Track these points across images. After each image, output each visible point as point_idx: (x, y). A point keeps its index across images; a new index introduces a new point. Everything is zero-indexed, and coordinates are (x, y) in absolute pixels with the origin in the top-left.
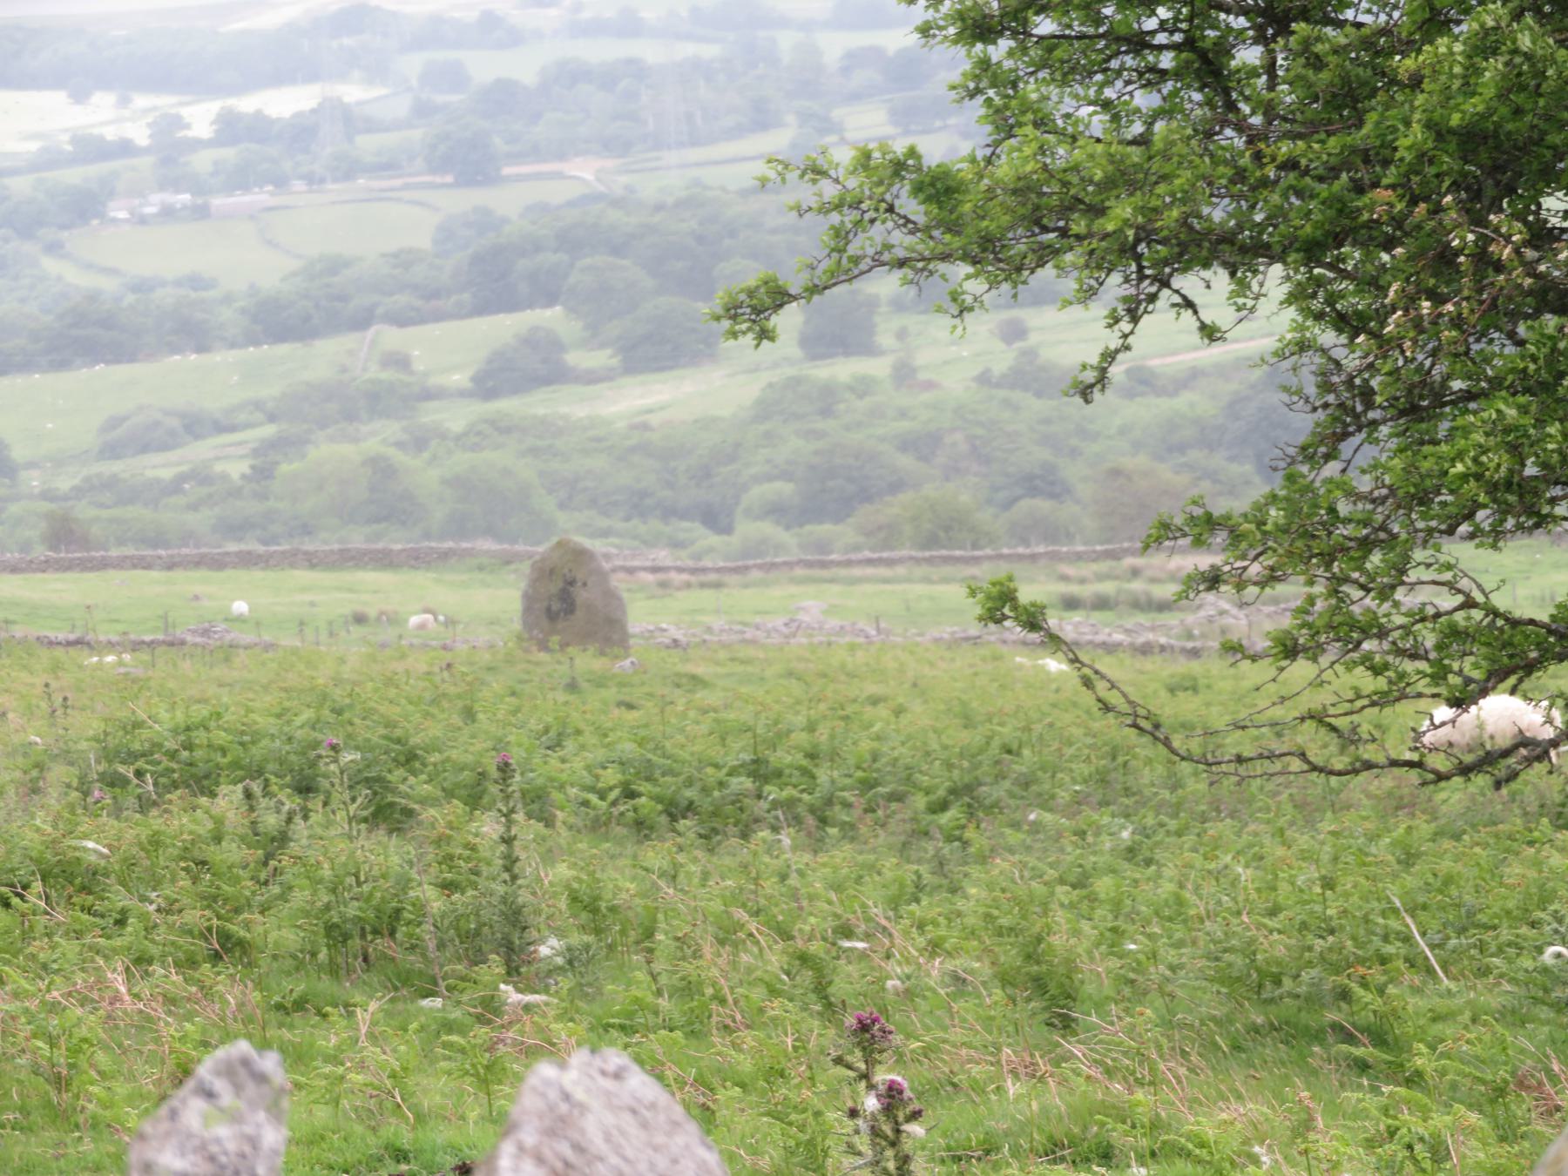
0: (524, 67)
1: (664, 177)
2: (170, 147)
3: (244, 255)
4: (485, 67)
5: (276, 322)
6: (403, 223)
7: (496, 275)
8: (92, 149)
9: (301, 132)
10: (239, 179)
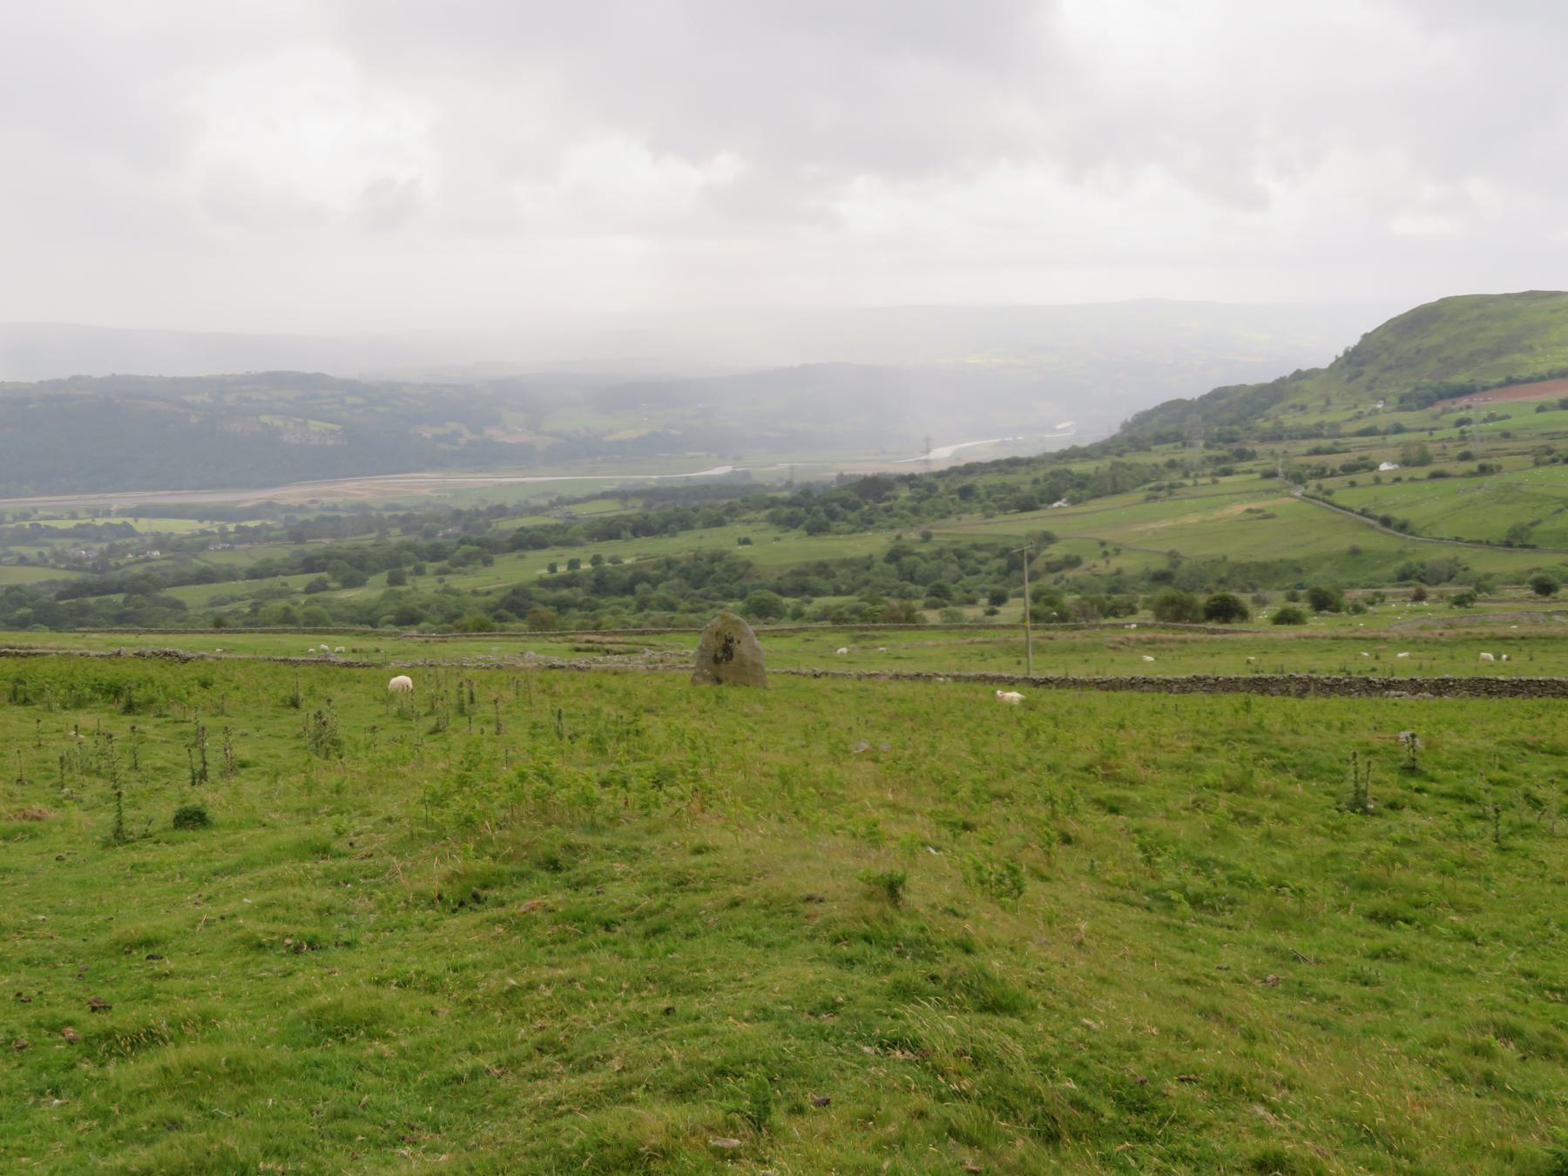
0: (311, 517)
1: (348, 542)
2: (224, 533)
3: (242, 559)
4: (300, 517)
5: (253, 574)
6: (281, 553)
7: (309, 565)
8: (203, 533)
9: (256, 530)
10: (241, 541)
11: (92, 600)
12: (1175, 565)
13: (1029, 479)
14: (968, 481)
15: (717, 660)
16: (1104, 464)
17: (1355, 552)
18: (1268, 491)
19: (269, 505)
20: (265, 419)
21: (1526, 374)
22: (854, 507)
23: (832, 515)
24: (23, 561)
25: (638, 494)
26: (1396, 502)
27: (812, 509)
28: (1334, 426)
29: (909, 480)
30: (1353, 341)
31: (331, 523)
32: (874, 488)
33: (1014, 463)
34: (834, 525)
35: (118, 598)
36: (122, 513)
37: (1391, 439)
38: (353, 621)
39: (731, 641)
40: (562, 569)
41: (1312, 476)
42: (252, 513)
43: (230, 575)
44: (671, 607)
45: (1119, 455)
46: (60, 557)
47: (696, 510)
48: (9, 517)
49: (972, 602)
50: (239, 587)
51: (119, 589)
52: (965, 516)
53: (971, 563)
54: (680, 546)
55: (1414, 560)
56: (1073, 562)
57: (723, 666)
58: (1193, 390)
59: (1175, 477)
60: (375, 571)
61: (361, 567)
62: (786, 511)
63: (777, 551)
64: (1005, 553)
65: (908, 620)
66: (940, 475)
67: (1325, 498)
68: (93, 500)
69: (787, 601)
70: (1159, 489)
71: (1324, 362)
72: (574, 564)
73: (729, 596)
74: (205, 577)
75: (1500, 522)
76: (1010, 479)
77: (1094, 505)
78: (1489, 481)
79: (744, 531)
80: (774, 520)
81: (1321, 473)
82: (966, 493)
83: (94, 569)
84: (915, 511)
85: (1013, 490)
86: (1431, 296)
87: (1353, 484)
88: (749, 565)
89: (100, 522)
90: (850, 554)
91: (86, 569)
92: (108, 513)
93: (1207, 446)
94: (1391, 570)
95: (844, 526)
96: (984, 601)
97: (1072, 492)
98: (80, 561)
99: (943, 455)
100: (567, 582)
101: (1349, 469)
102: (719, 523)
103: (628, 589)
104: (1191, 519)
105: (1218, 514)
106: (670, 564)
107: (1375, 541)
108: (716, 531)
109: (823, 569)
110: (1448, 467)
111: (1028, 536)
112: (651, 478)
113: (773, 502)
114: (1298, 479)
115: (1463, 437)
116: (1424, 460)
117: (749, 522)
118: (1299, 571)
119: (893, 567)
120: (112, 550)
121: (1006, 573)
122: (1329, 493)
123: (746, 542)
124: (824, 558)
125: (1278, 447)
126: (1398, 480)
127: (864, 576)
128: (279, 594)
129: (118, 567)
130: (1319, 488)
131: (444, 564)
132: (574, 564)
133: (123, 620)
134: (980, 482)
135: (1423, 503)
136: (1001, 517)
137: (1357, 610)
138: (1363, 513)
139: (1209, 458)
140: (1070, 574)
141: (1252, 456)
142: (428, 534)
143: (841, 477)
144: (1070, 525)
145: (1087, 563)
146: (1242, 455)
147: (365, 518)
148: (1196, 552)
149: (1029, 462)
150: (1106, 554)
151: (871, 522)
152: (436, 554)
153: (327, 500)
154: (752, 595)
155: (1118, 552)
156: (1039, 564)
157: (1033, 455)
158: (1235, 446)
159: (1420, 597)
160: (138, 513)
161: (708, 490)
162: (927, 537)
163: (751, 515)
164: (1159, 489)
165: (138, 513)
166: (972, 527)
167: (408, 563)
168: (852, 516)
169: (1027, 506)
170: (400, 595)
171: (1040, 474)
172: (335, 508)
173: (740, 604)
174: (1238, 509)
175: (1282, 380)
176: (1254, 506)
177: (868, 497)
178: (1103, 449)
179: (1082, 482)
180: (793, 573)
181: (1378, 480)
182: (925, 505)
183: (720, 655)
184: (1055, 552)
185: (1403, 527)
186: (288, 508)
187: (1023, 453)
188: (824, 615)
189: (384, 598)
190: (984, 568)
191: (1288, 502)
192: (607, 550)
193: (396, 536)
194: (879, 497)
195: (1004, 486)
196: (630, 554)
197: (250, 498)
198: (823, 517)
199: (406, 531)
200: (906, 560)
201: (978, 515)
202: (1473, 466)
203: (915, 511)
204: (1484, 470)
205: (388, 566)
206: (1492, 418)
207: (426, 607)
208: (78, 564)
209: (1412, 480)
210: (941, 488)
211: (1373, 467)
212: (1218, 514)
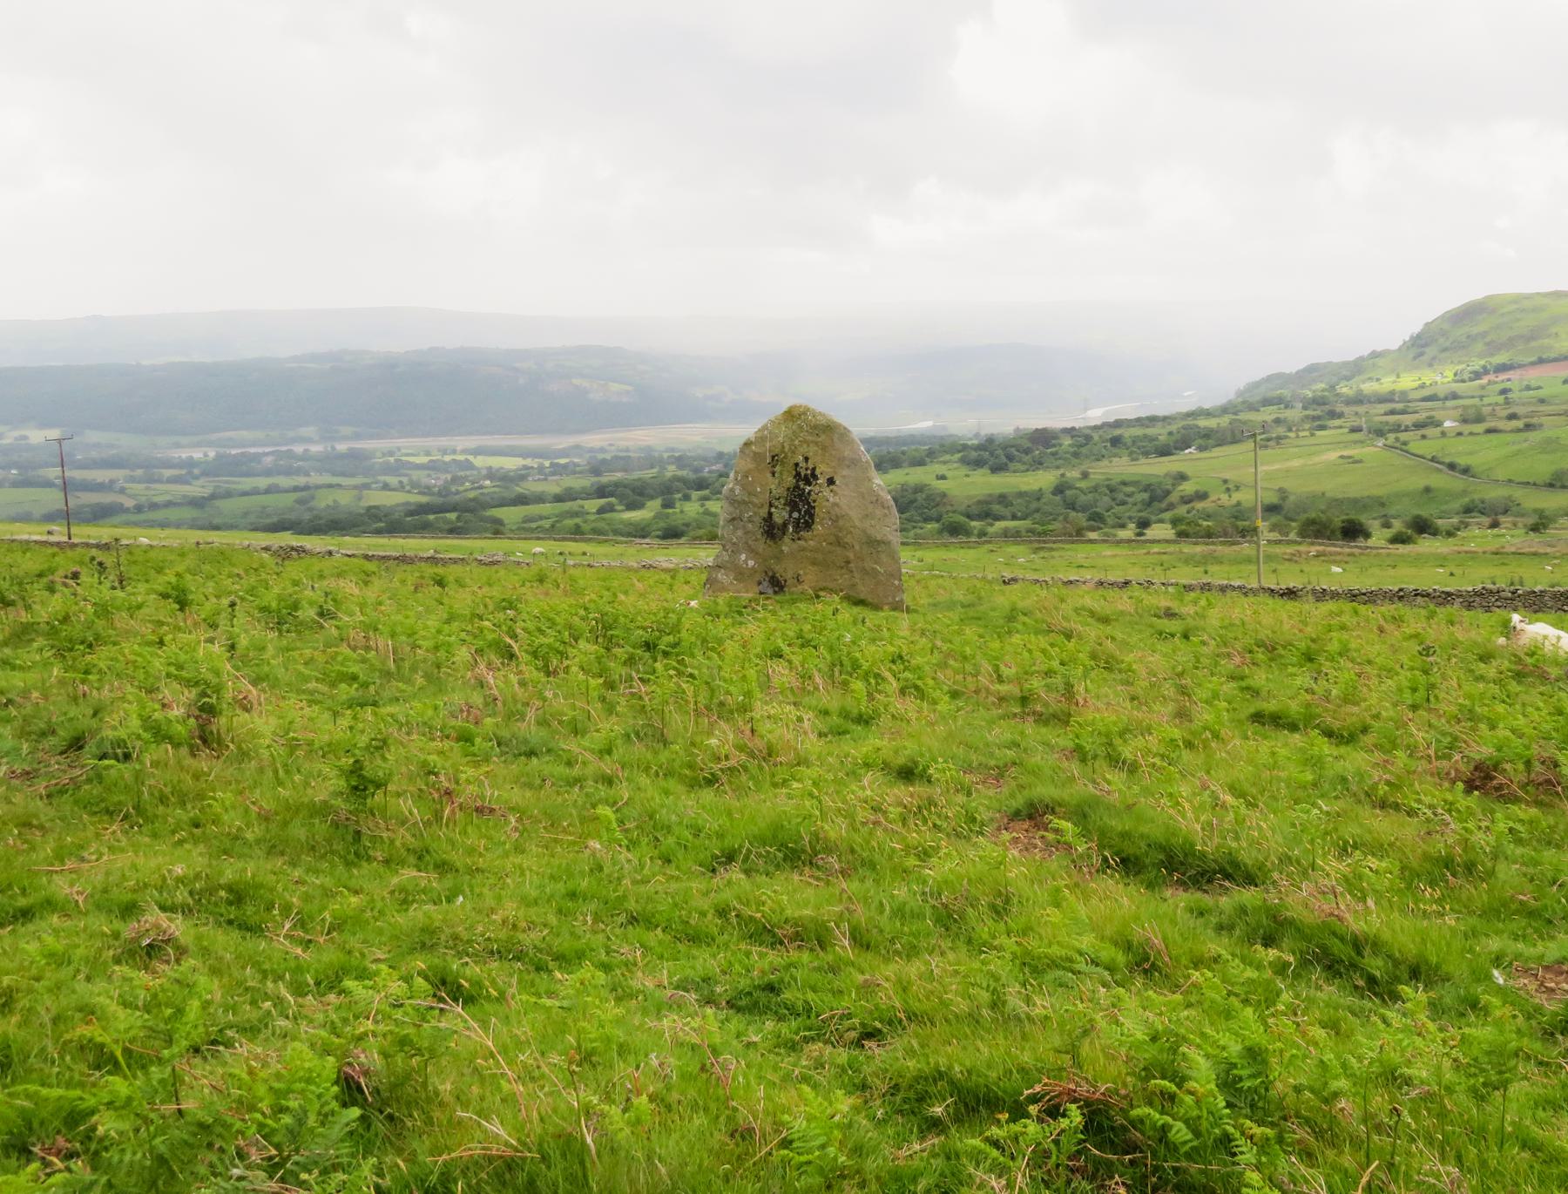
0: (608, 457)
1: (636, 475)
3: (553, 488)
4: (600, 456)
5: (558, 499)
7: (601, 492)
8: (526, 467)
9: (565, 466)
10: (553, 474)
11: (431, 517)
12: (1284, 499)
13: (1164, 431)
14: (1117, 432)
15: (772, 531)
16: (1225, 421)
17: (1427, 490)
18: (1355, 442)
19: (577, 447)
20: (576, 381)
21: (1553, 355)
22: (1027, 451)
23: (1010, 458)
24: (386, 487)
26: (1459, 451)
27: (992, 454)
28: (1404, 393)
29: (1070, 431)
30: (1417, 328)
31: (623, 462)
32: (1043, 438)
33: (1153, 420)
34: (1012, 466)
35: (452, 516)
36: (464, 451)
37: (1449, 404)
38: (629, 535)
39: (811, 478)
41: (1390, 431)
43: (540, 499)
45: (1235, 414)
46: (414, 485)
47: (903, 453)
48: (379, 454)
49: (1123, 526)
50: (546, 509)
51: (454, 509)
52: (1115, 460)
53: (1120, 496)
55: (1476, 497)
56: (1202, 496)
57: (787, 546)
58: (1292, 366)
59: (1281, 430)
60: (652, 498)
61: (641, 494)
62: (974, 454)
63: (967, 486)
64: (1147, 488)
65: (1077, 535)
66: (1096, 428)
67: (1402, 448)
68: (444, 442)
69: (973, 523)
70: (1269, 440)
71: (1394, 343)
73: (927, 520)
74: (521, 500)
75: (1544, 467)
76: (1150, 431)
77: (1217, 452)
78: (1535, 436)
80: (965, 461)
81: (1397, 428)
82: (1116, 441)
83: (440, 494)
84: (1076, 455)
85: (1153, 439)
86: (1475, 293)
87: (1424, 437)
88: (944, 495)
89: (447, 458)
90: (1024, 488)
91: (432, 494)
92: (454, 452)
93: (1305, 408)
94: (1457, 505)
95: (1019, 466)
96: (1132, 526)
97: (1200, 441)
98: (428, 487)
99: (1096, 415)
101: (1419, 426)
102: (921, 463)
104: (1295, 463)
105: (1316, 459)
107: (1442, 481)
108: (919, 469)
109: (1002, 499)
110: (1501, 425)
111: (1166, 475)
113: (965, 447)
114: (1380, 433)
115: (1507, 402)
116: (1479, 419)
117: (945, 463)
118: (1383, 505)
119: (1058, 498)
120: (455, 480)
121: (1149, 504)
122: (1405, 443)
123: (943, 477)
124: (1004, 491)
125: (1361, 409)
126: (1460, 434)
127: (1034, 505)
128: (576, 514)
129: (458, 493)
130: (1397, 439)
131: (707, 492)
133: (454, 531)
134: (1128, 433)
135: (1482, 452)
136: (1143, 460)
137: (1450, 534)
138: (1433, 459)
139: (1307, 417)
140: (1199, 505)
141: (1341, 415)
142: (697, 470)
143: (1018, 429)
144: (1200, 468)
145: (1213, 497)
146: (1333, 415)
147: (651, 460)
148: (1299, 488)
149: (1165, 419)
150: (1228, 490)
151: (1041, 463)
152: (701, 485)
153: (623, 444)
154: (946, 519)
155: (1237, 488)
156: (1174, 497)
157: (1166, 413)
158: (1327, 408)
159: (1495, 525)
160: (477, 452)
161: (912, 439)
162: (1085, 475)
163: (947, 457)
164: (1269, 440)
165: (477, 452)
166: (1121, 467)
167: (678, 491)
168: (1027, 458)
169: (1164, 452)
170: (667, 516)
171: (1174, 428)
172: (627, 450)
173: (937, 526)
174: (1333, 456)
175: (1362, 358)
176: (1345, 453)
177: (1037, 446)
178: (1224, 410)
179: (1207, 434)
180: (979, 502)
181: (1443, 434)
182: (1084, 450)
183: (780, 515)
184: (1188, 488)
185: (1466, 471)
186: (591, 450)
187: (1161, 413)
188: (1006, 534)
189: (655, 517)
190: (1130, 500)
191: (1372, 451)
193: (671, 471)
194: (1047, 446)
195: (1145, 436)
198: (1004, 459)
199: (681, 467)
200: (1068, 493)
201: (1125, 459)
202: (1520, 424)
203: (1076, 455)
204: (1528, 427)
205: (663, 493)
206: (1528, 388)
207: (687, 525)
208: (427, 490)
209: (1471, 434)
210: (1096, 438)
211: (1439, 424)
212: (1316, 459)
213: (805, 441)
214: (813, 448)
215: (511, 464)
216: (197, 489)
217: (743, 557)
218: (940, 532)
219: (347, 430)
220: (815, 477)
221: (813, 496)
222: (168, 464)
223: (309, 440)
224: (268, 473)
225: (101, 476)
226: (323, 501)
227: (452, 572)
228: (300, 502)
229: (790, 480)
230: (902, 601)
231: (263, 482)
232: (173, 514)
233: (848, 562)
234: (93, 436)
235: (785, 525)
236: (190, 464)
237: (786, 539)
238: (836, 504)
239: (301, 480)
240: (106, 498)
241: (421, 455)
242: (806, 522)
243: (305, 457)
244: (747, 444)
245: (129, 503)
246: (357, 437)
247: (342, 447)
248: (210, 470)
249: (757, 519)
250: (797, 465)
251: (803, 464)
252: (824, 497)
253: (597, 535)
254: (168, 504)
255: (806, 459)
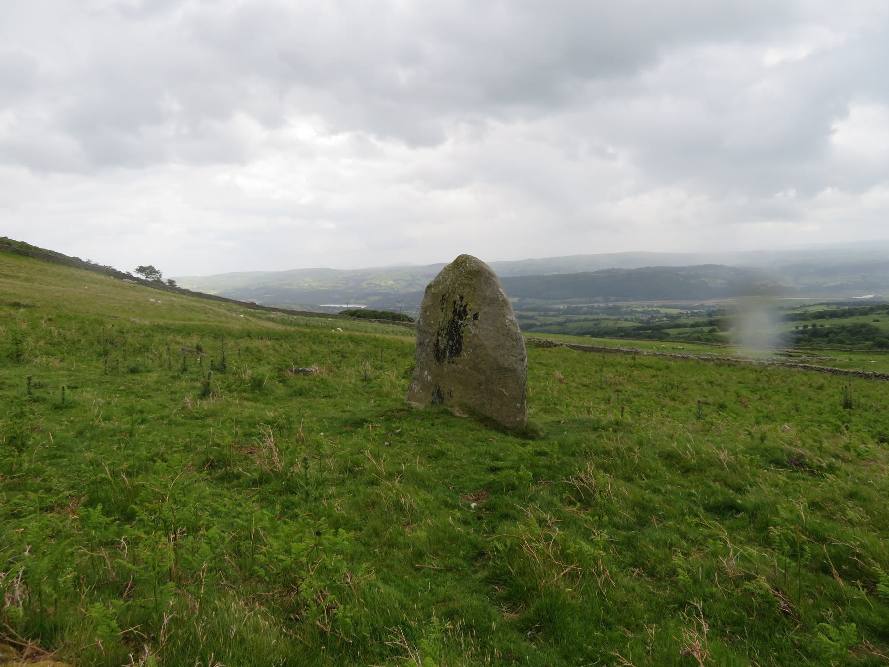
3: (691, 321)
5: (693, 326)
6: (706, 319)
15: (439, 355)
25: (833, 304)
35: (650, 331)
39: (461, 314)
40: (801, 328)
42: (696, 308)
43: (685, 326)
44: (841, 342)
46: (636, 319)
50: (688, 329)
51: (649, 328)
54: (848, 321)
68: (649, 303)
72: (805, 326)
74: (678, 326)
79: (876, 317)
88: (877, 329)
100: (802, 332)
102: (864, 313)
103: (826, 335)
106: (843, 327)
108: (865, 317)
112: (841, 299)
123: (877, 321)
128: (700, 332)
132: (805, 326)
133: (650, 338)
160: (661, 307)
161: (862, 303)
163: (880, 311)
192: (819, 322)
196: (828, 324)
197: (696, 304)
208: (641, 321)
213: (462, 284)
214: (467, 290)
215: (675, 312)
216: (560, 319)
217: (426, 373)
218: (873, 346)
219: (613, 298)
220: (465, 313)
221: (462, 329)
222: (551, 310)
223: (599, 302)
224: (585, 314)
225: (531, 314)
226: (603, 324)
227: (609, 358)
228: (595, 324)
229: (451, 315)
230: (522, 421)
231: (582, 317)
232: (553, 328)
233: (480, 384)
234: (528, 300)
235: (445, 350)
236: (559, 310)
237: (446, 362)
238: (475, 336)
239: (596, 317)
240: (531, 322)
241: (640, 308)
242: (456, 350)
243: (598, 308)
244: (429, 287)
245: (538, 323)
246: (617, 301)
247: (611, 305)
248: (565, 312)
249: (431, 345)
250: (455, 302)
251: (459, 303)
252: (471, 329)
253: (708, 341)
254: (551, 324)
255: (462, 298)
